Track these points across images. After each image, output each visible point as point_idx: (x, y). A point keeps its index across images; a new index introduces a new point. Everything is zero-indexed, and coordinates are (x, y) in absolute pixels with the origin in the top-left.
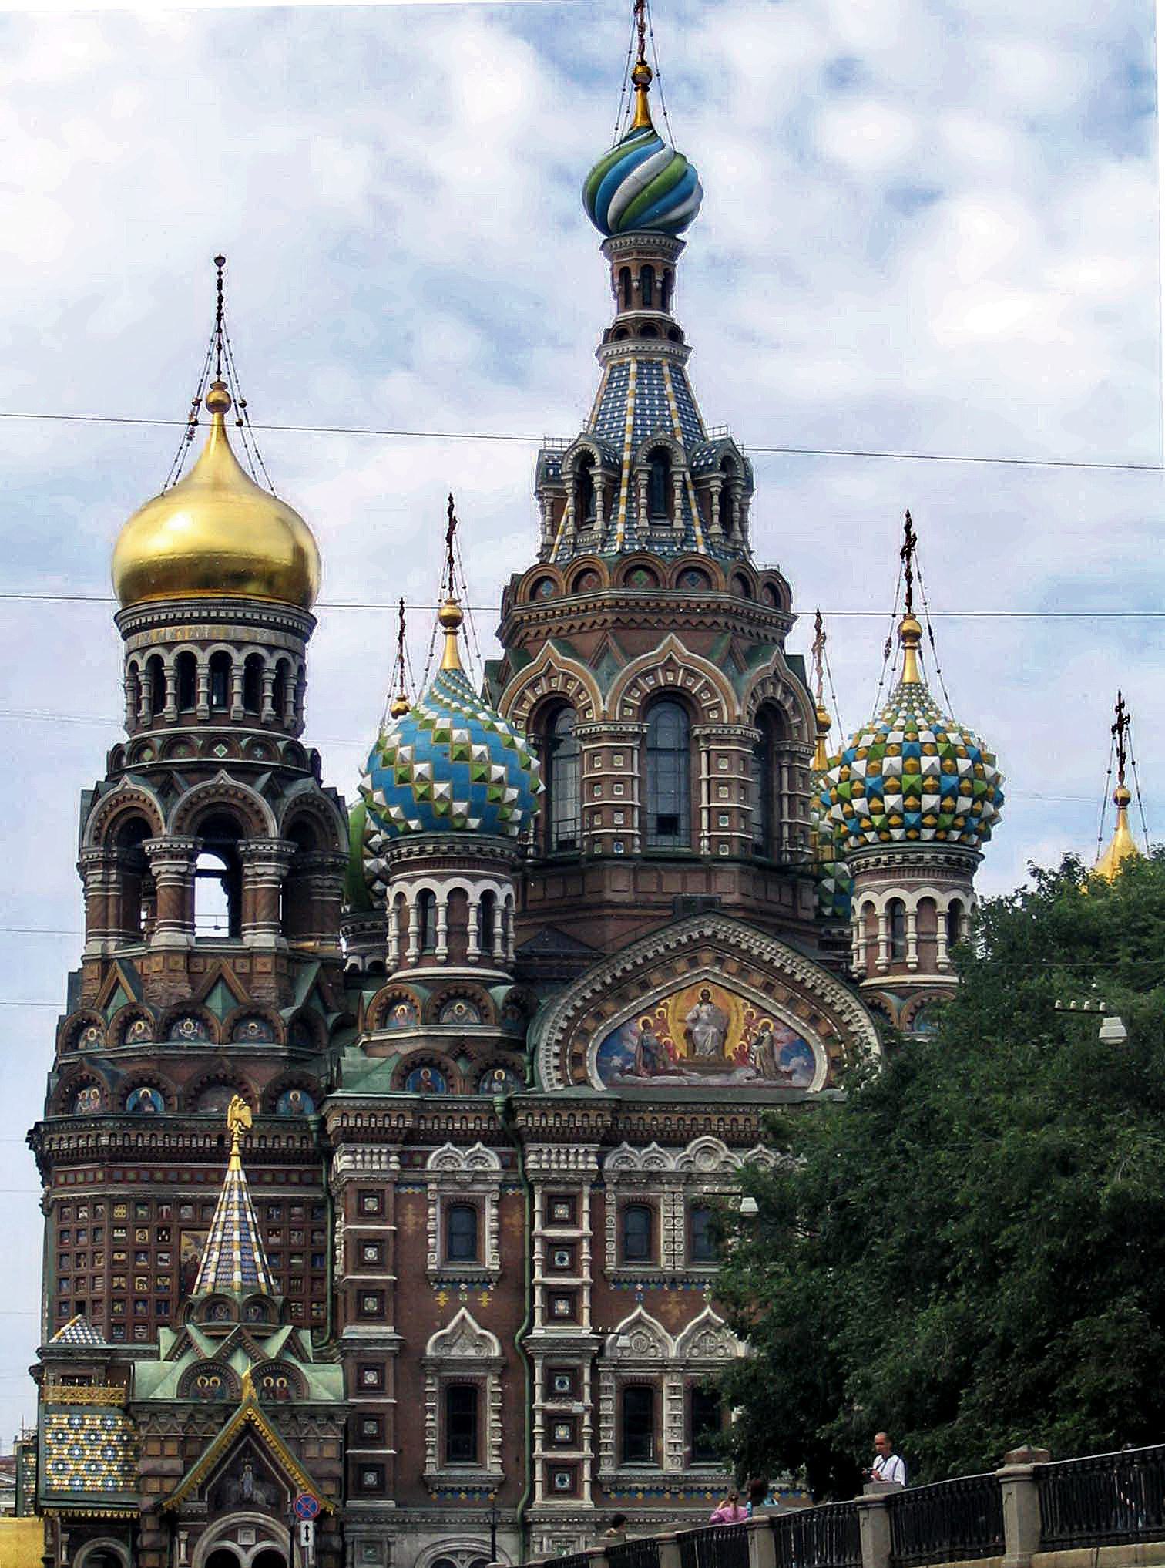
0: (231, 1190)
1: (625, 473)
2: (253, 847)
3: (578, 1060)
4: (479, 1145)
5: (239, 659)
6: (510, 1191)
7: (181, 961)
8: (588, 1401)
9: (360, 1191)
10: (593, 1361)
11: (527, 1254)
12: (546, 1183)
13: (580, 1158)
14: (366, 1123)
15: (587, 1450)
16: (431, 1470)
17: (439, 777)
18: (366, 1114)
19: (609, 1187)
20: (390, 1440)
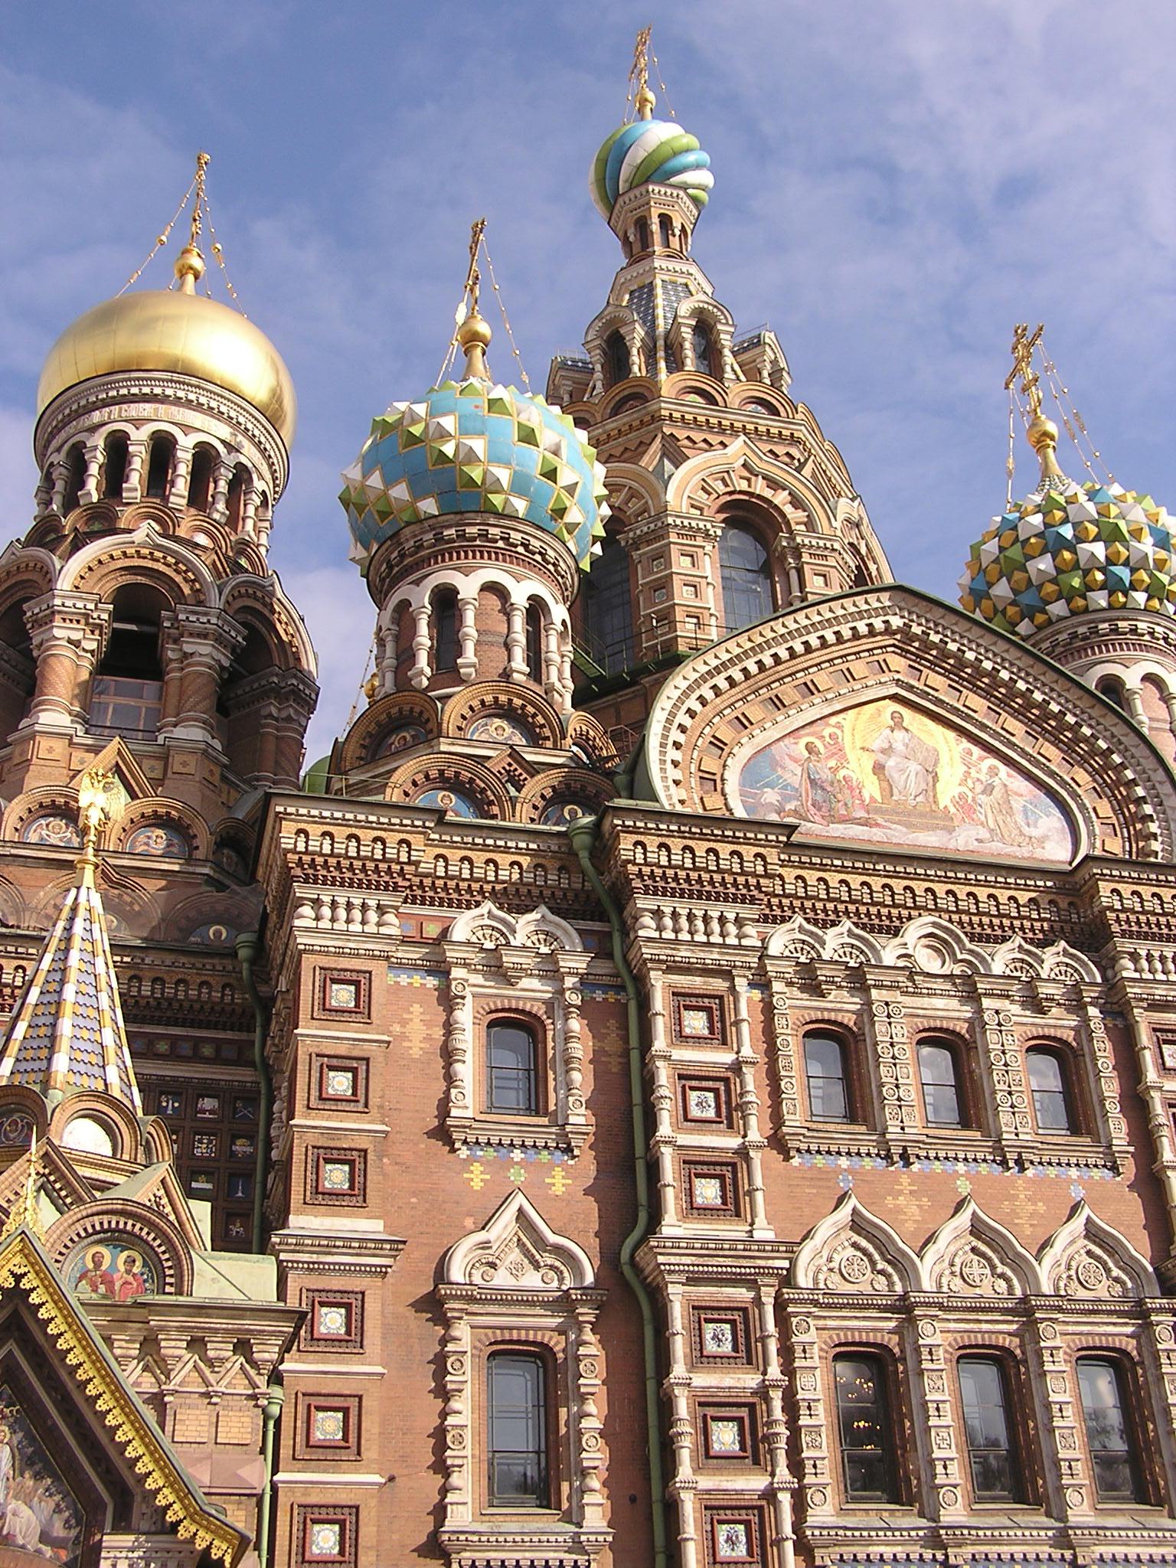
1: (661, 343)
2: (182, 617)
3: (712, 781)
5: (186, 443)
6: (599, 996)
8: (774, 1371)
10: (778, 1296)
11: (637, 1097)
12: (674, 968)
13: (732, 928)
15: (783, 1472)
16: (461, 1516)
17: (464, 431)
19: (777, 986)
20: (371, 1450)
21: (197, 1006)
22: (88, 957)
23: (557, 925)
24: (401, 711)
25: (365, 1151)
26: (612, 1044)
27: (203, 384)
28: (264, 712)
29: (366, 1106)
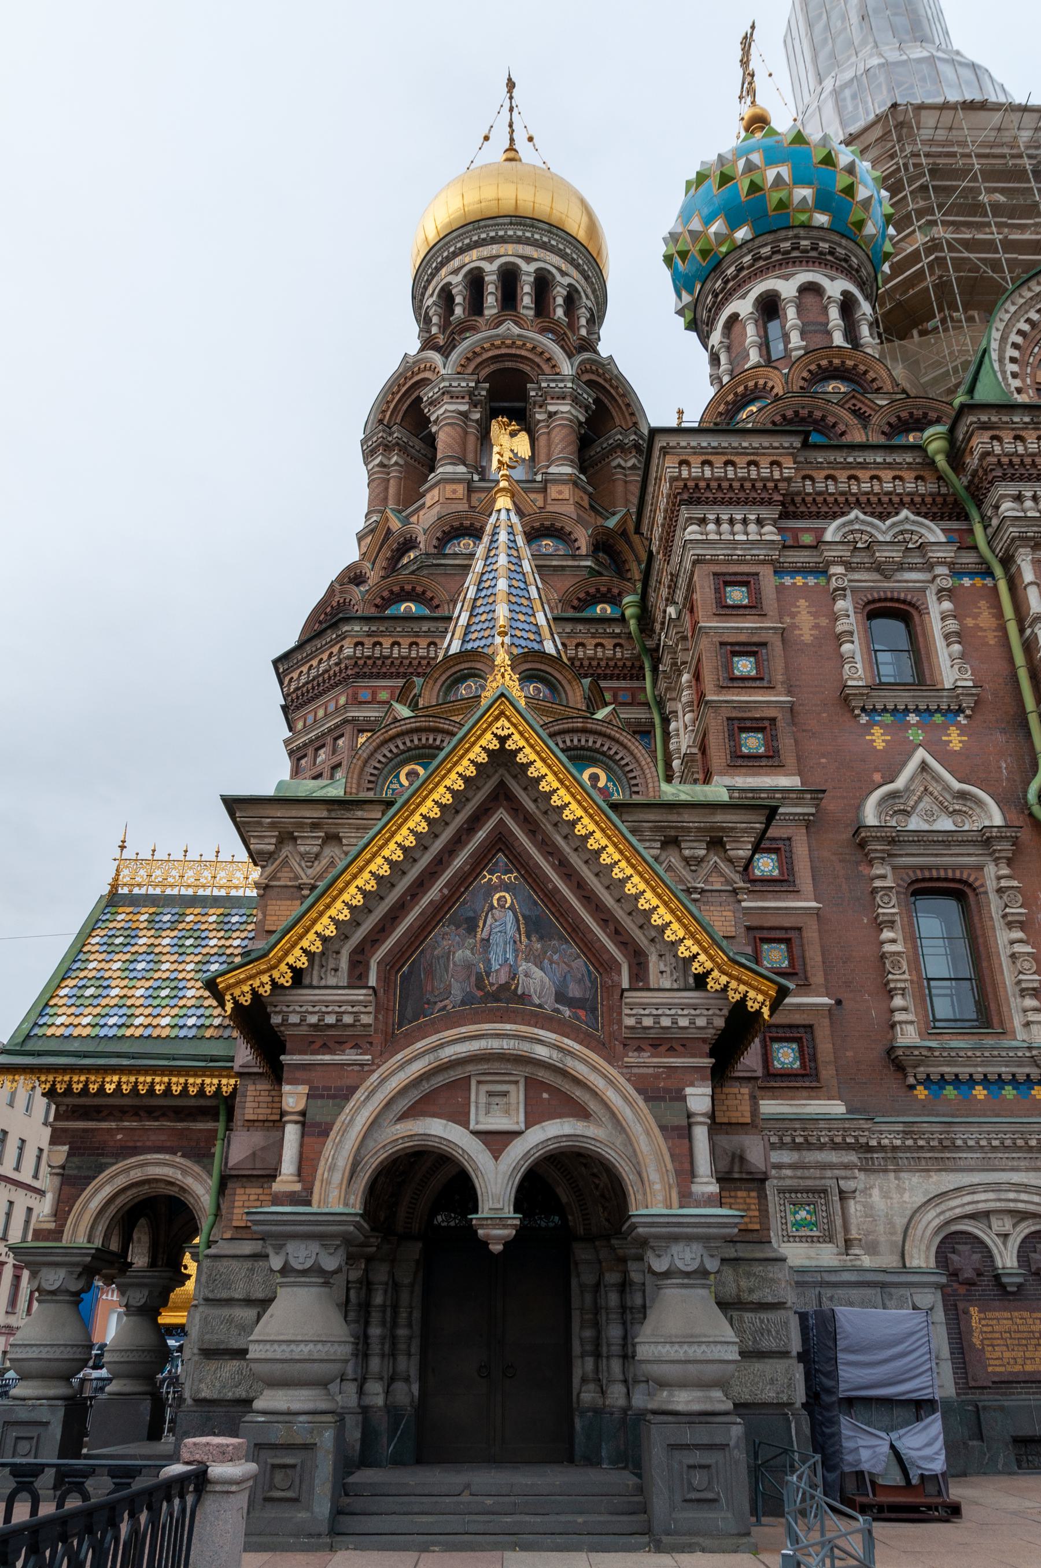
0: (494, 534)
2: (544, 385)
4: (905, 513)
5: (528, 269)
6: (967, 582)
7: (461, 490)
9: (715, 574)
14: (719, 472)
18: (718, 461)
20: (817, 978)
21: (594, 663)
22: (514, 560)
23: (921, 524)
24: (746, 388)
25: (773, 720)
26: (985, 619)
27: (536, 223)
28: (614, 464)
29: (770, 682)
